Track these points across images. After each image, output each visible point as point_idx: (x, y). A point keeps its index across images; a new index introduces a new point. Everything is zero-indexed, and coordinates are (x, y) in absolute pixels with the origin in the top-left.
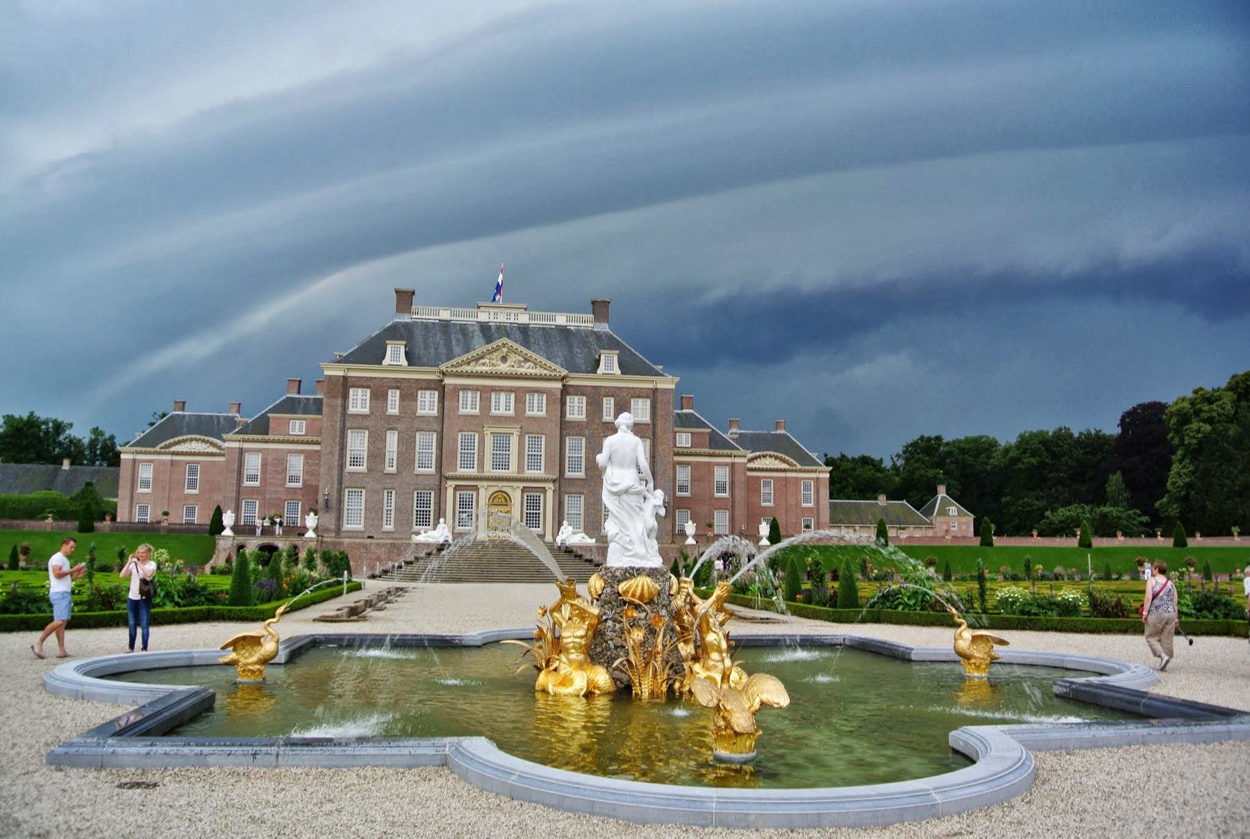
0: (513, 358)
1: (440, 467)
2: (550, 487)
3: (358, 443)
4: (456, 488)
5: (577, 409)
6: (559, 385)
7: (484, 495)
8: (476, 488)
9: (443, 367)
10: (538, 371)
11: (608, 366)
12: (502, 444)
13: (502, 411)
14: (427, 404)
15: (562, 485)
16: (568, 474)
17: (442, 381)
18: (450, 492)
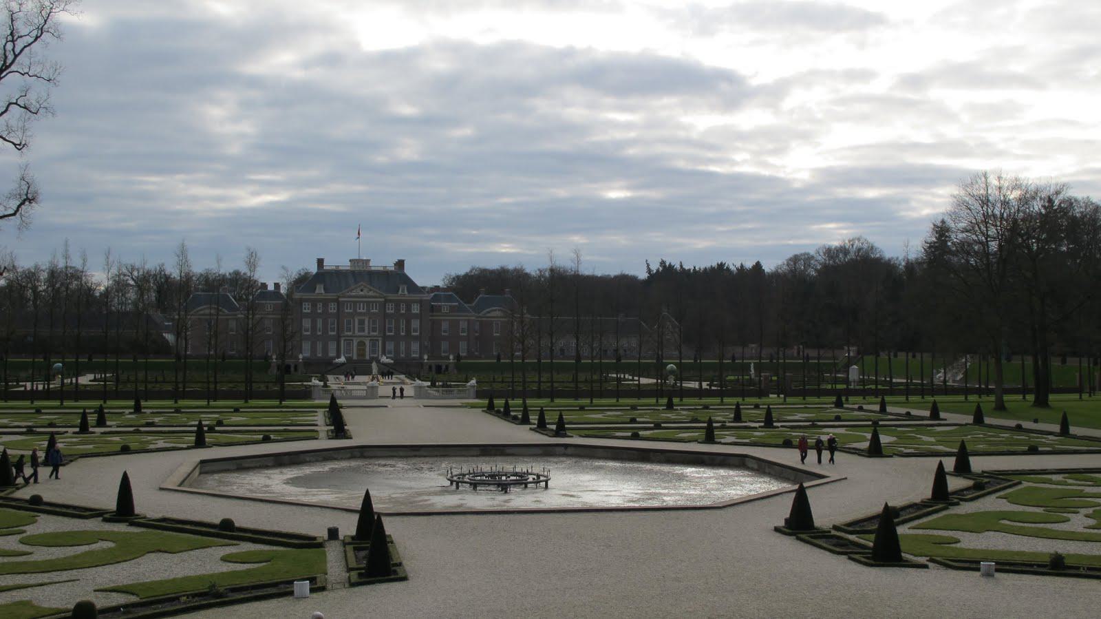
0: (365, 290)
1: (338, 333)
2: (380, 339)
3: (307, 323)
4: (345, 340)
5: (390, 310)
6: (383, 300)
7: (355, 344)
8: (352, 340)
9: (338, 294)
10: (375, 294)
11: (403, 291)
12: (361, 322)
13: (361, 310)
14: (333, 308)
15: (386, 339)
16: (388, 334)
17: (338, 299)
18: (342, 342)
